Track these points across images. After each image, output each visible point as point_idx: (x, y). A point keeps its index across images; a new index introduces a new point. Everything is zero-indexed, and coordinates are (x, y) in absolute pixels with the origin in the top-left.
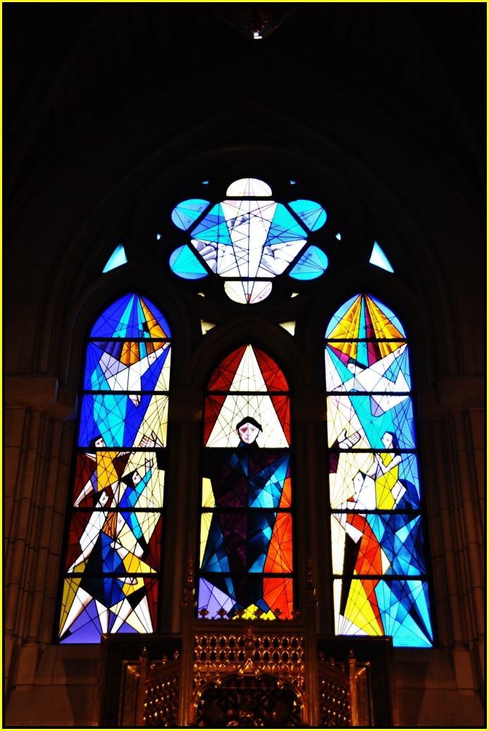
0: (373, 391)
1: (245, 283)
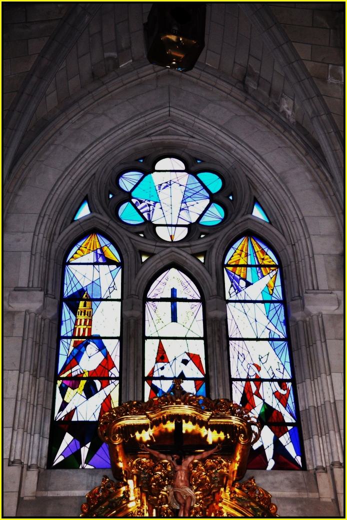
0: (257, 300)
1: (170, 228)
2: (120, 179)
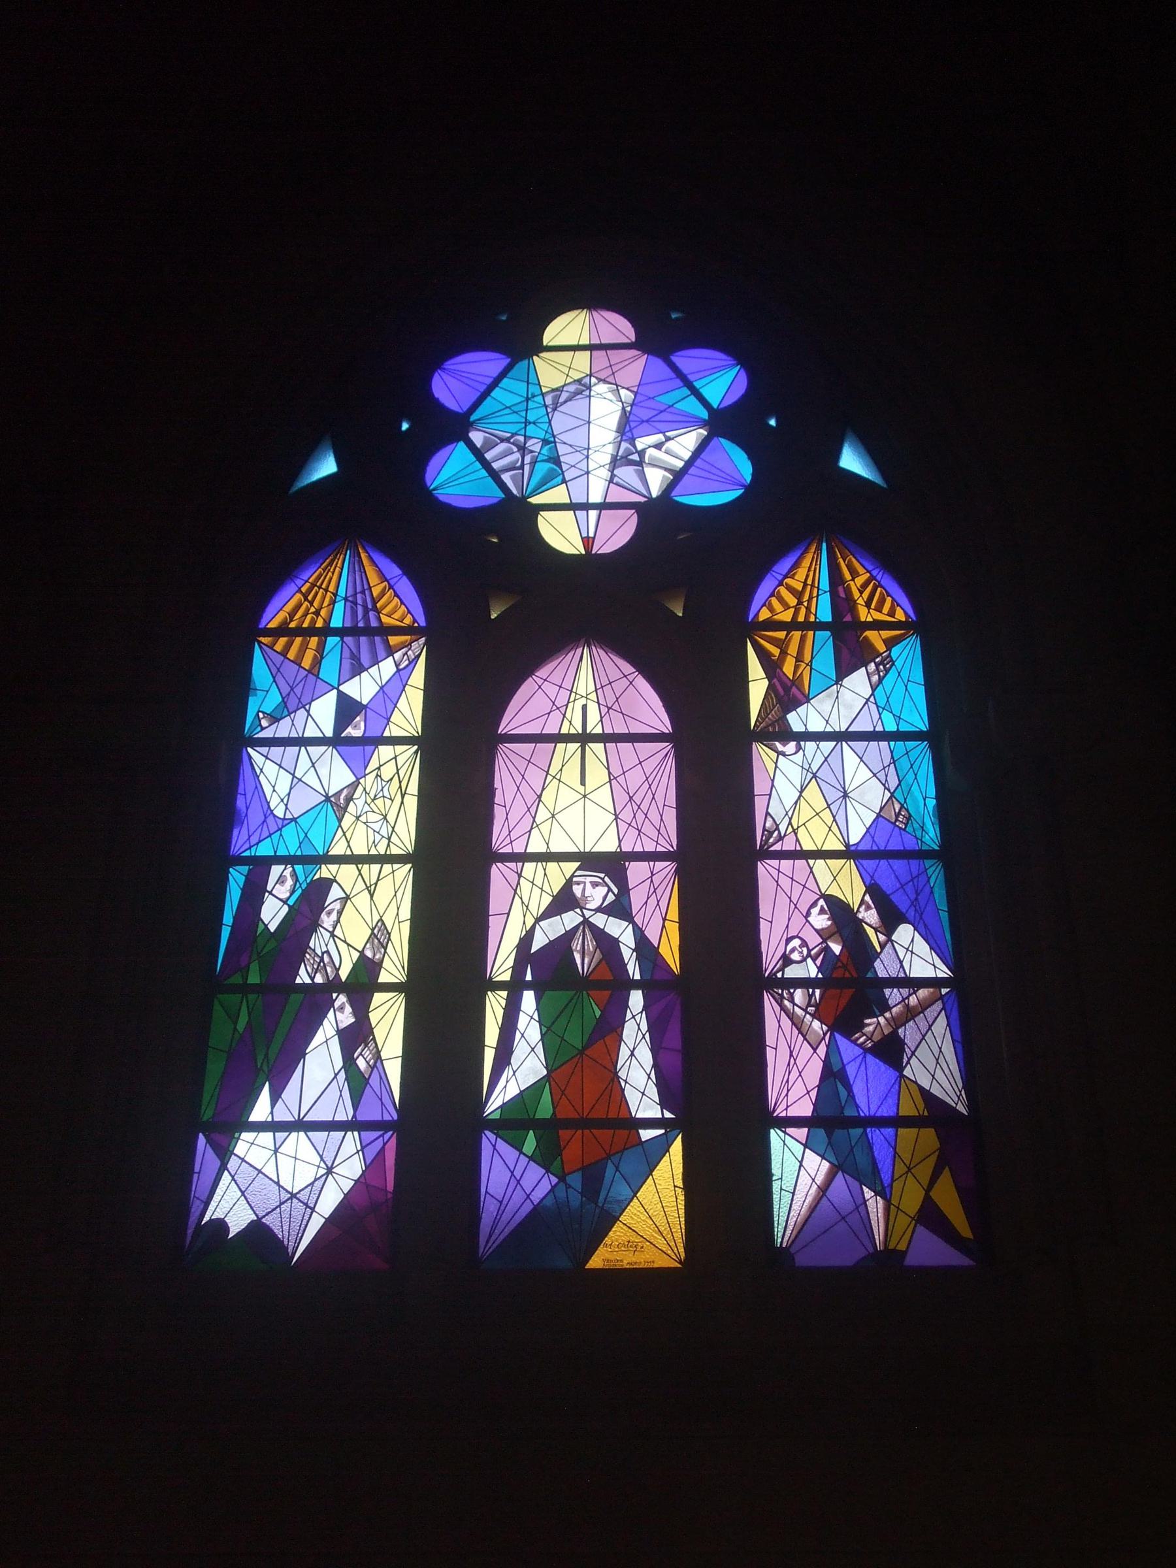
1: (581, 514)
2: (436, 374)
